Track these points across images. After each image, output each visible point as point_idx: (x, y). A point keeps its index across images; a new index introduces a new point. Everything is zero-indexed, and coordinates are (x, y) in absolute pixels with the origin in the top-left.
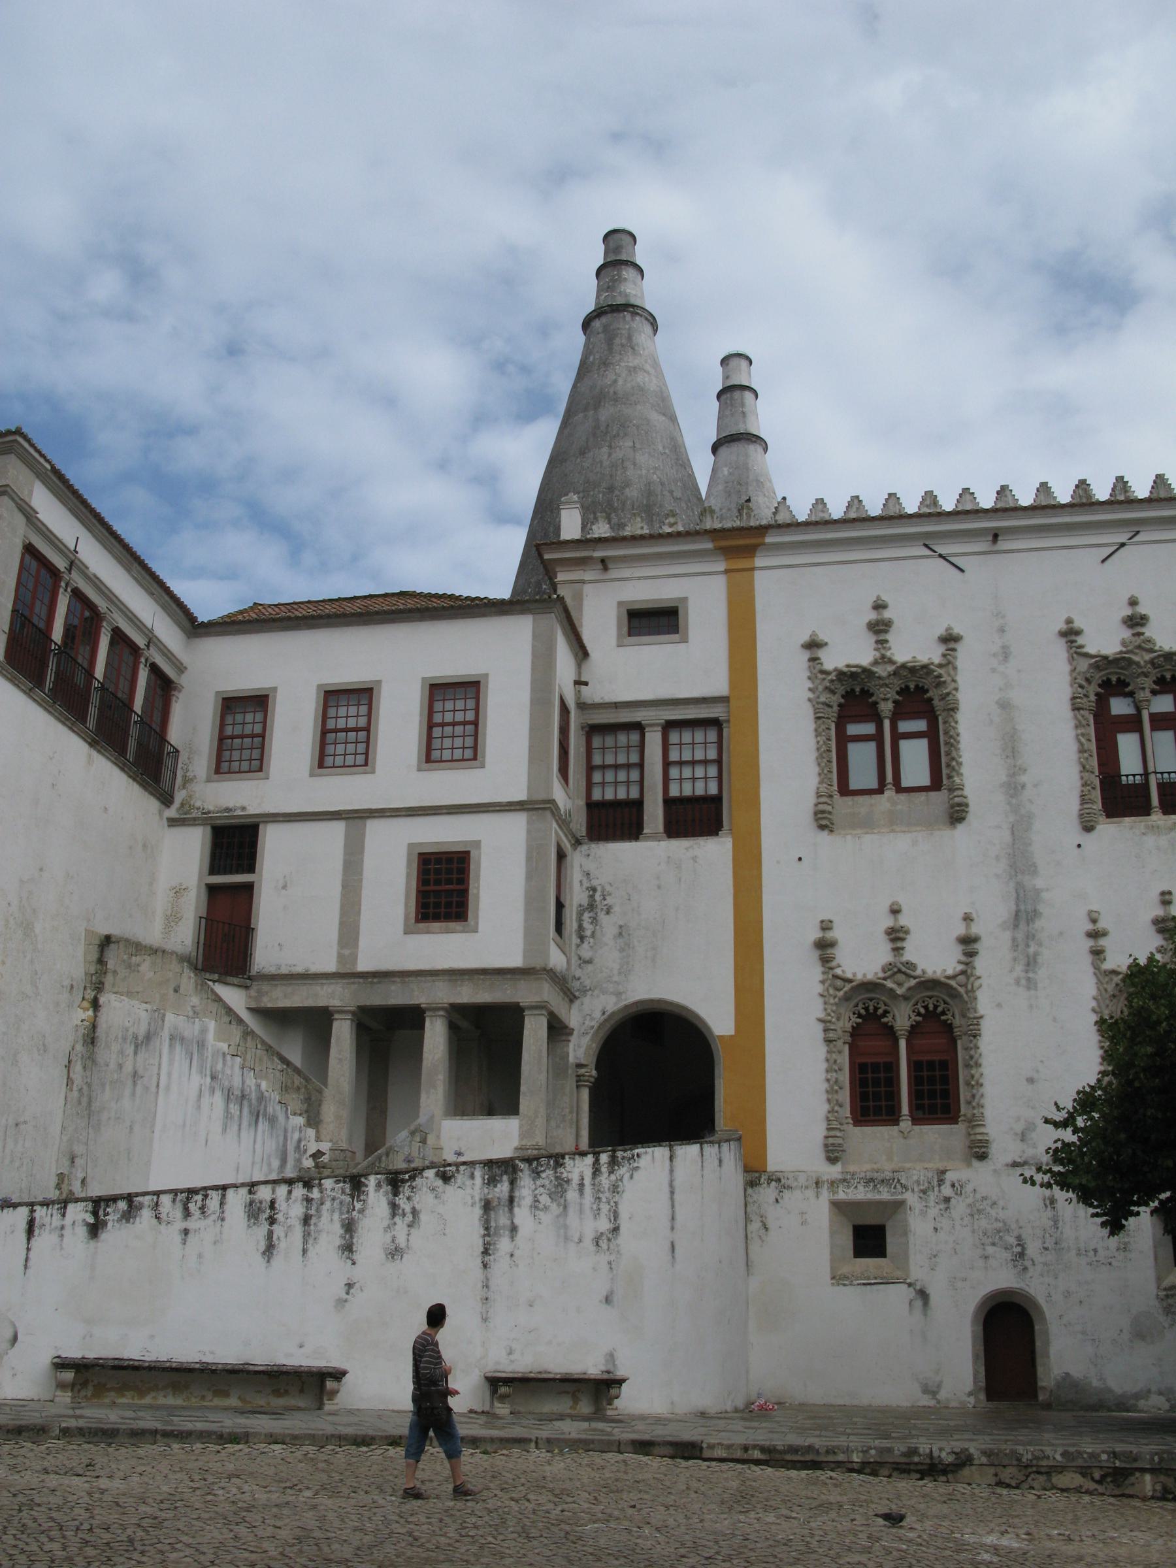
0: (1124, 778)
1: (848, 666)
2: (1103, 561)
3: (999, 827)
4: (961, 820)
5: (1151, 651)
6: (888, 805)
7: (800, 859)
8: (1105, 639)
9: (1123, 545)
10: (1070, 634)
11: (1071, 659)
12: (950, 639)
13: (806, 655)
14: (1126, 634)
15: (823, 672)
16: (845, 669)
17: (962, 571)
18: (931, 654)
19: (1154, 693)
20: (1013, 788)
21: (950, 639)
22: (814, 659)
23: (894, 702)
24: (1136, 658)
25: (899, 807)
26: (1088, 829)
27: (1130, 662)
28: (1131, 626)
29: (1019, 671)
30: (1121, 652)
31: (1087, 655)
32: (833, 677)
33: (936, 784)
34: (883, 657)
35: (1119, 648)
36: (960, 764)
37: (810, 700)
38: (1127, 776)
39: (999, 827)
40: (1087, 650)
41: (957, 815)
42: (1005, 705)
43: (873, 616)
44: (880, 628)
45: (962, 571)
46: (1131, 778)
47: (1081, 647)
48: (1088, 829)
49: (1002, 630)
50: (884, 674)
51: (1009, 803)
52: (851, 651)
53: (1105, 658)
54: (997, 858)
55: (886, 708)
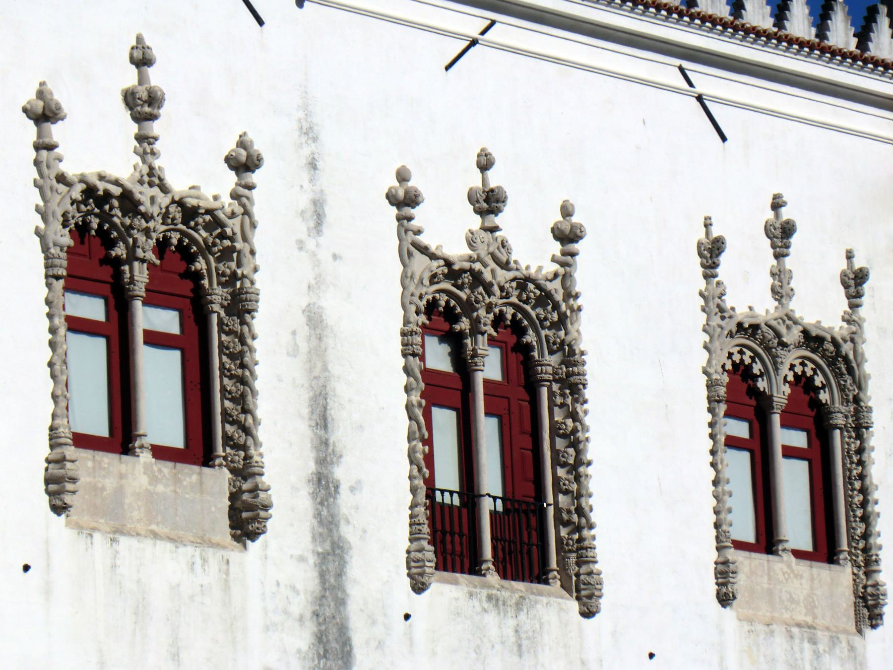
0: (438, 493)
1: (102, 178)
2: (447, 68)
3: (302, 559)
4: (253, 536)
5: (505, 266)
6: (144, 480)
7: (26, 568)
8: (448, 229)
9: (474, 42)
10: (405, 201)
11: (405, 257)
12: (244, 163)
13: (30, 130)
14: (476, 222)
15: (61, 179)
16: (101, 186)
17: (260, 22)
18: (215, 186)
19: (492, 342)
20: (324, 486)
21: (244, 163)
22: (44, 146)
23: (151, 266)
24: (487, 276)
25: (160, 488)
26: (419, 587)
27: (477, 279)
28: (480, 212)
29: (335, 257)
30: (471, 260)
31: (424, 250)
32: (76, 193)
33: (199, 448)
34: (151, 172)
35: (465, 251)
36: (256, 421)
37: (37, 232)
38: (442, 492)
39: (302, 559)
40: (423, 239)
41: (246, 520)
42: (315, 320)
43: (130, 77)
44: (143, 106)
45: (260, 22)
46: (447, 495)
47: (418, 232)
48: (419, 587)
49: (313, 165)
50: (155, 210)
51: (318, 515)
52: (97, 148)
53: (448, 263)
54: (301, 619)
55: (141, 275)
